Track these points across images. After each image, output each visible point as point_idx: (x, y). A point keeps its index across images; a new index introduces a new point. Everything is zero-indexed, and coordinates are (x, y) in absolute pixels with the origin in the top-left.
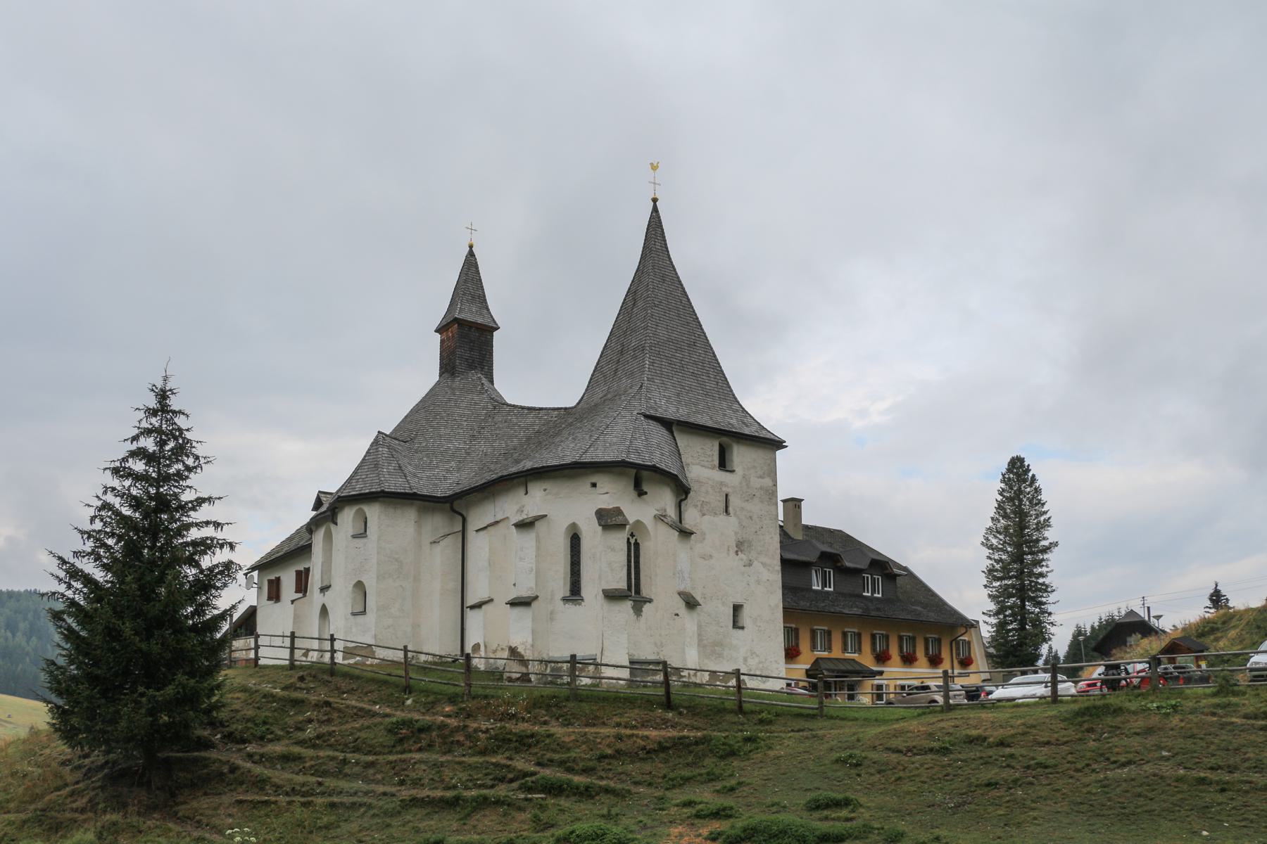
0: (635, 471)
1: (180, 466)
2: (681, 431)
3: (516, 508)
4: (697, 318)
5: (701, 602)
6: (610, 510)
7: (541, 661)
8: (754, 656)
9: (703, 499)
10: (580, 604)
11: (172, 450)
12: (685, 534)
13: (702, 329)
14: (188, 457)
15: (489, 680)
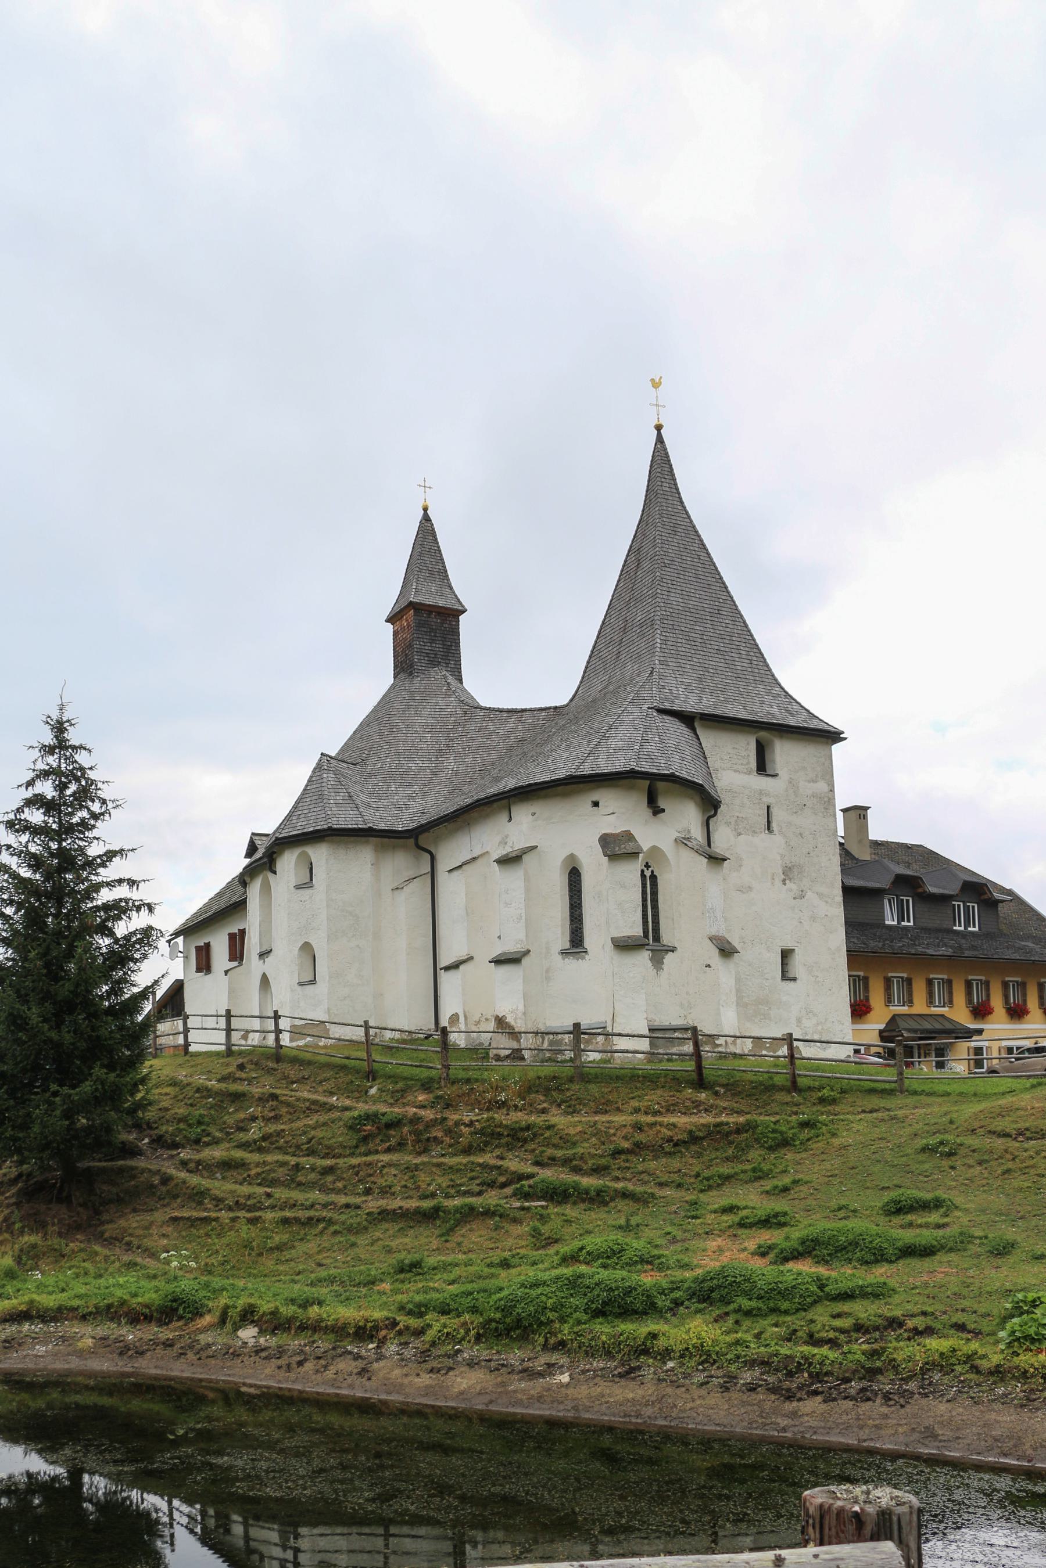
0: (648, 782)
1: (84, 814)
2: (704, 726)
3: (498, 839)
4: (721, 578)
5: (738, 947)
6: (617, 835)
7: (537, 1033)
9: (737, 814)
10: (583, 958)
11: (74, 794)
12: (716, 860)
13: (728, 592)
14: (93, 801)
15: (472, 1059)
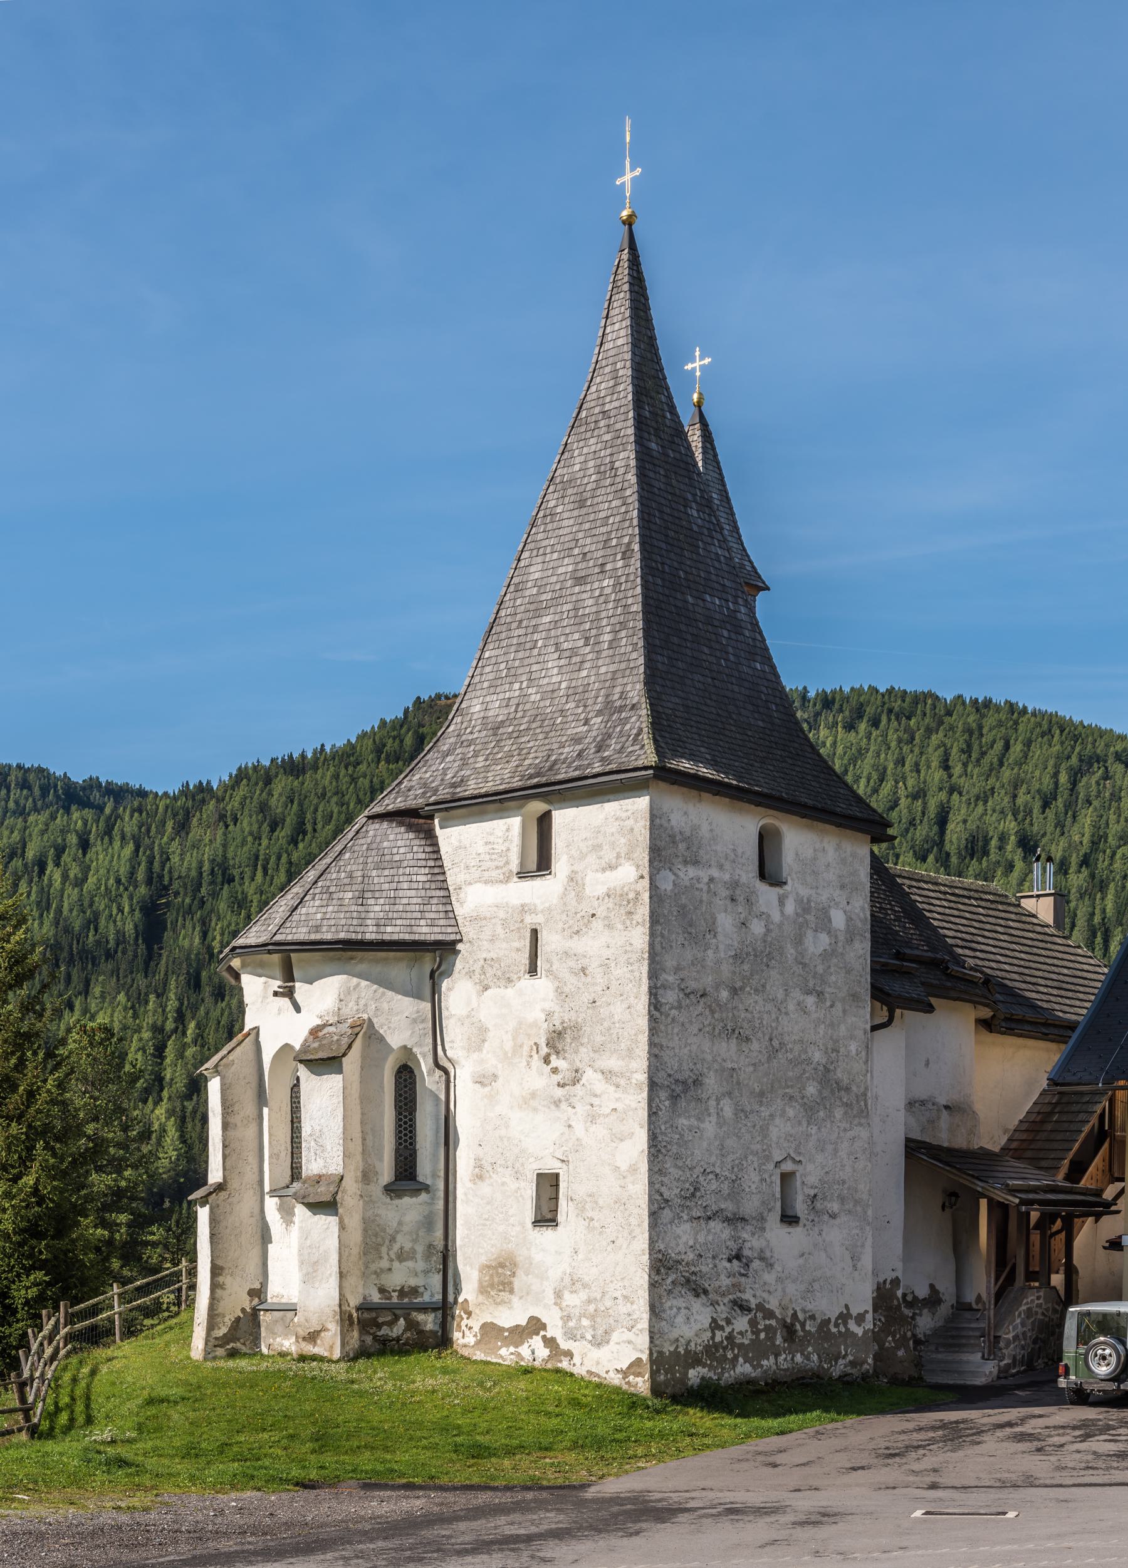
8: (578, 1285)
9: (484, 956)
